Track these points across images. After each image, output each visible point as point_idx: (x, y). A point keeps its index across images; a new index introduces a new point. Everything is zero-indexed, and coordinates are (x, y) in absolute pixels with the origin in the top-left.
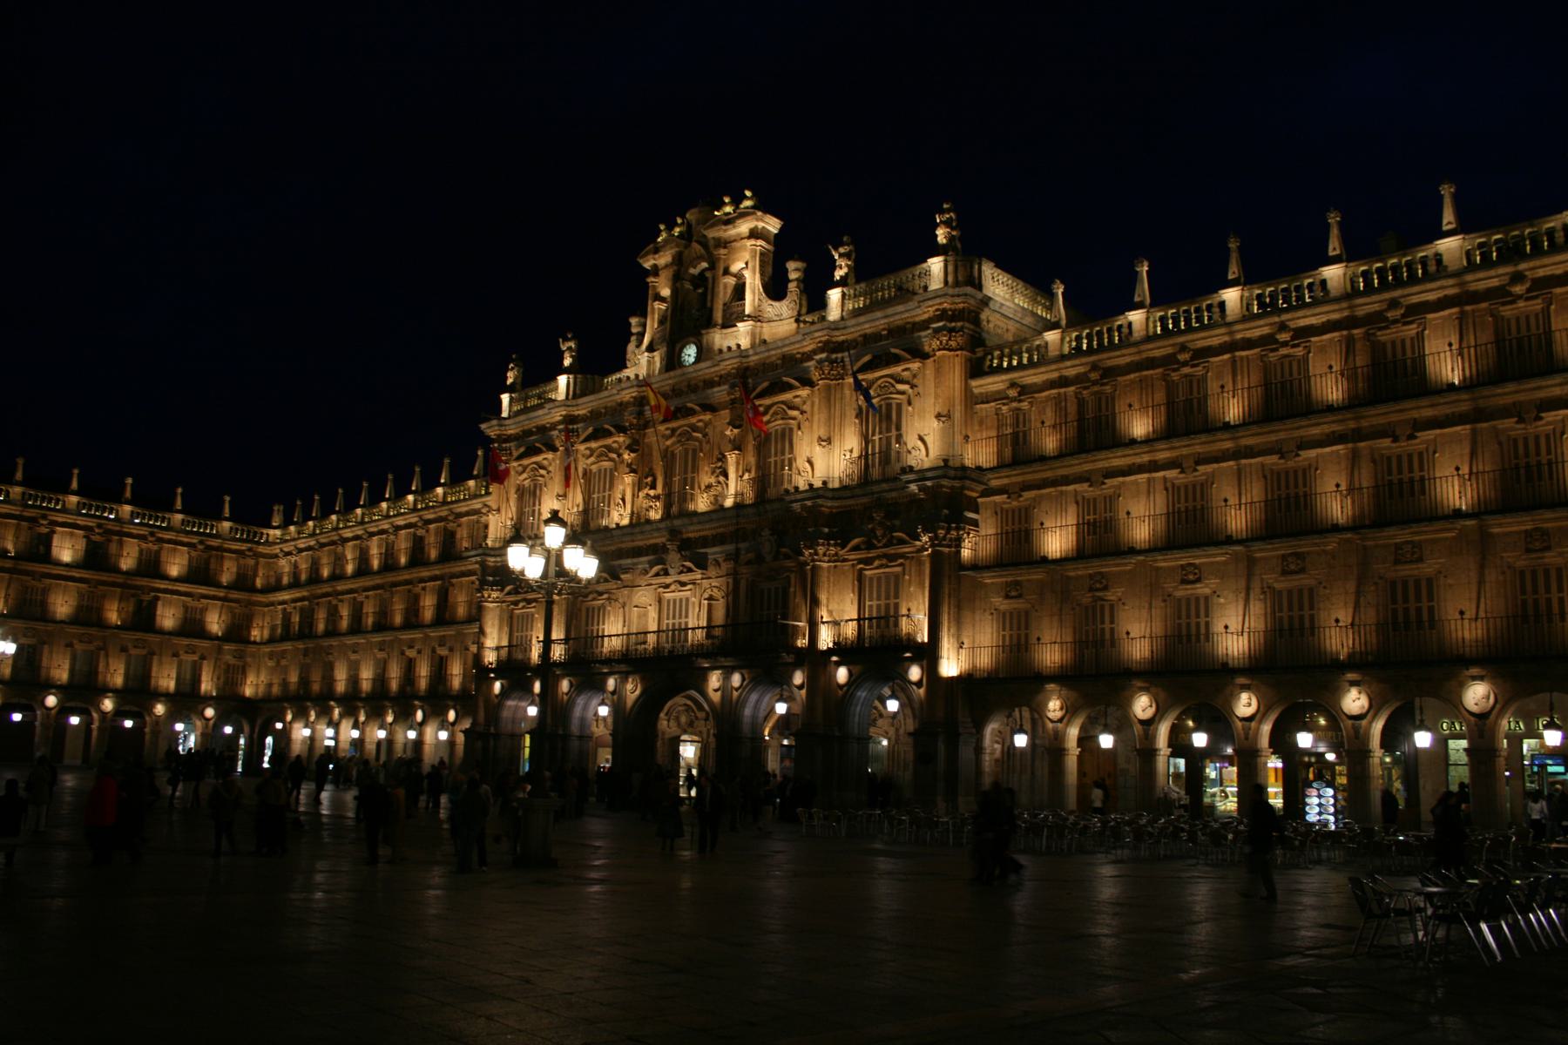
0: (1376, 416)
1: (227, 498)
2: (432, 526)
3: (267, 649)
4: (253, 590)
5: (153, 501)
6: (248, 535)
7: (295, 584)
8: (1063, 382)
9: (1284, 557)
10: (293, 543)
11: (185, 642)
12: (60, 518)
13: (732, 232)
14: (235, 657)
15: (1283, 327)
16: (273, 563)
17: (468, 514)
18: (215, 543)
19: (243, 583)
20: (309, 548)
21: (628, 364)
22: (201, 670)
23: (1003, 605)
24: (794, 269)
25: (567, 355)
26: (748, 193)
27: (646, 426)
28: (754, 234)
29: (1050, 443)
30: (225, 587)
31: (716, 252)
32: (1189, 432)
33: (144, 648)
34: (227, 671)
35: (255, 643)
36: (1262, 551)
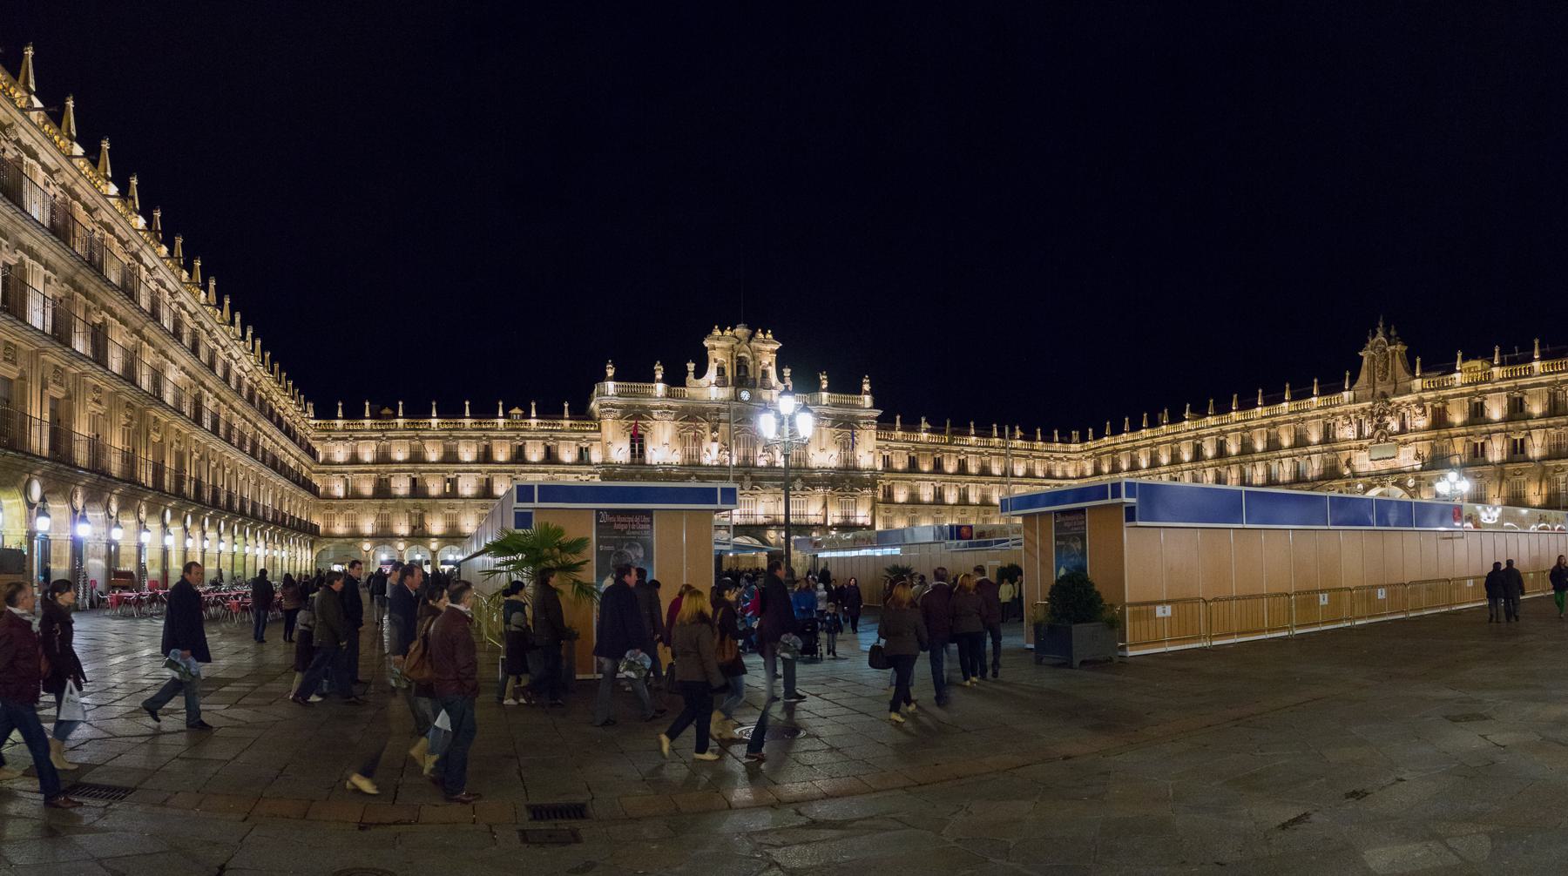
0: (983, 479)
2: (528, 442)
8: (902, 449)
9: (962, 510)
13: (763, 347)
15: (962, 450)
17: (563, 439)
21: (687, 384)
23: (885, 514)
24: (787, 372)
25: (657, 372)
26: (769, 331)
27: (719, 421)
28: (772, 352)
29: (900, 467)
31: (756, 354)
32: (938, 473)
36: (956, 508)
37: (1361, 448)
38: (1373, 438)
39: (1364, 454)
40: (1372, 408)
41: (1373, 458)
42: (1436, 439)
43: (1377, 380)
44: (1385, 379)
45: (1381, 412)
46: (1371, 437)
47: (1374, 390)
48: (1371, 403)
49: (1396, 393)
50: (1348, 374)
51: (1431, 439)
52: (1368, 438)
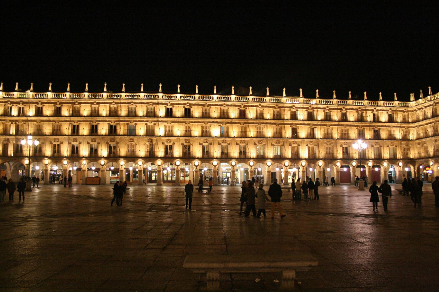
1: (395, 94)
3: (417, 142)
4: (408, 123)
5: (373, 98)
6: (404, 105)
7: (425, 118)
10: (422, 105)
11: (390, 142)
12: (348, 107)
14: (406, 145)
16: (414, 113)
18: (394, 109)
19: (405, 121)
20: (430, 105)
22: (396, 150)
30: (400, 123)
33: (378, 145)
34: (404, 150)
35: (412, 140)
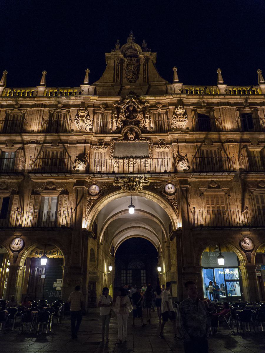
37: (101, 143)
38: (120, 132)
39: (102, 150)
40: (119, 104)
41: (117, 155)
42: (203, 141)
43: (125, 80)
44: (135, 81)
45: (131, 108)
46: (118, 131)
47: (121, 89)
48: (118, 99)
49: (147, 93)
50: (88, 71)
51: (197, 142)
52: (115, 133)
